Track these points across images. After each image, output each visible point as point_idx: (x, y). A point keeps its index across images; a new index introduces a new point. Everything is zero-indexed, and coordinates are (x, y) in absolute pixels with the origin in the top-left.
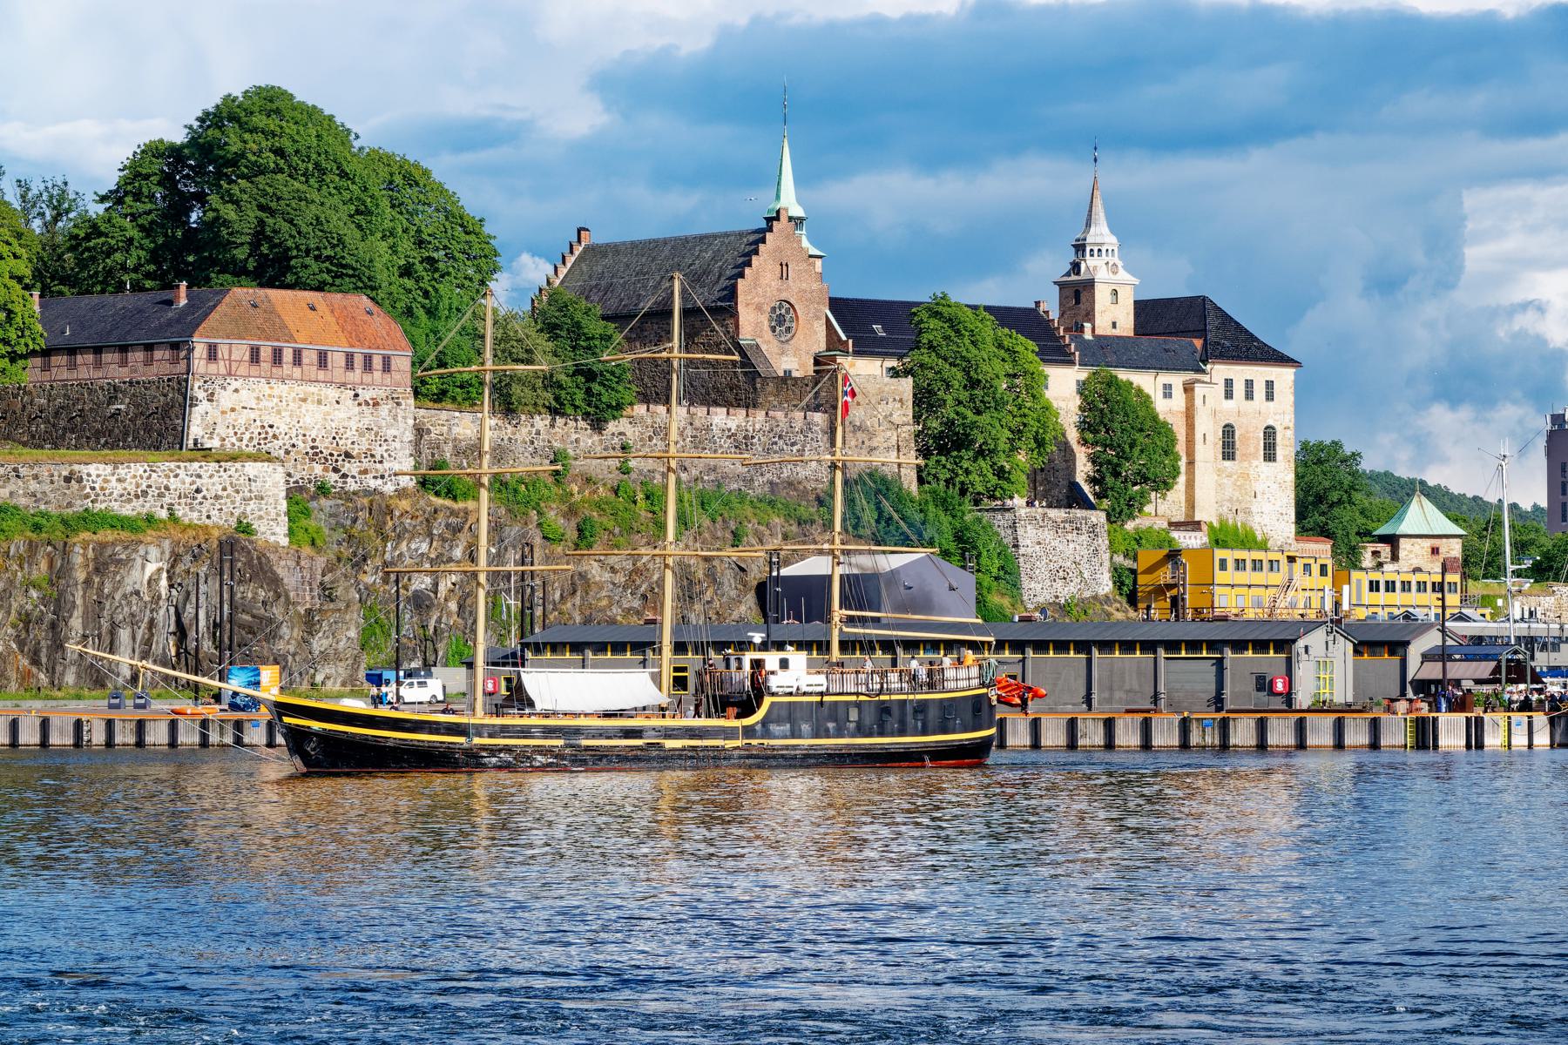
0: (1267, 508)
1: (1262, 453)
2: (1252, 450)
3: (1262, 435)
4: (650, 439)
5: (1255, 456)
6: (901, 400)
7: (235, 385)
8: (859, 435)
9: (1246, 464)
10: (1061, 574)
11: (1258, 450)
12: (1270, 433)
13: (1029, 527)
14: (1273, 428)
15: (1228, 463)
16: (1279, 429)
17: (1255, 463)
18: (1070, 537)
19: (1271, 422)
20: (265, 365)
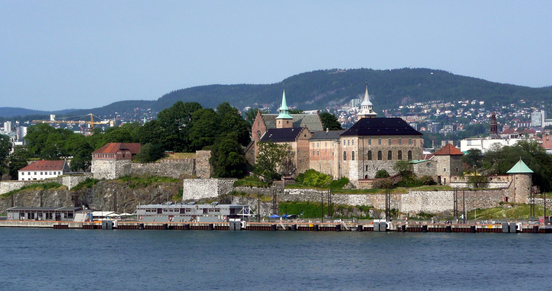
0: (352, 172)
1: (351, 158)
2: (349, 157)
3: (351, 154)
4: (162, 166)
5: (350, 160)
6: (208, 156)
7: (97, 161)
8: (199, 163)
9: (348, 161)
10: (196, 193)
11: (350, 157)
12: (353, 153)
13: (187, 183)
14: (354, 152)
15: (344, 161)
16: (355, 152)
17: (350, 161)
18: (201, 185)
19: (353, 150)
20: (100, 158)
